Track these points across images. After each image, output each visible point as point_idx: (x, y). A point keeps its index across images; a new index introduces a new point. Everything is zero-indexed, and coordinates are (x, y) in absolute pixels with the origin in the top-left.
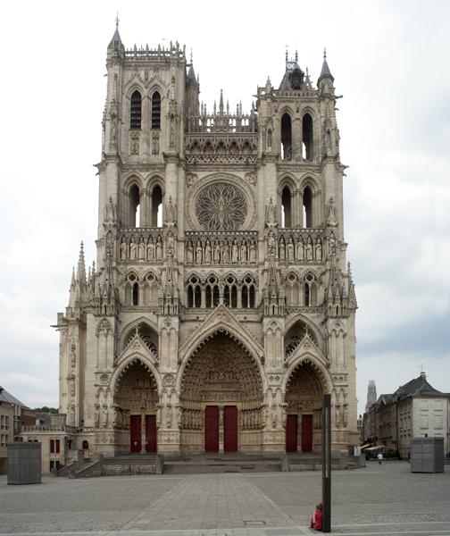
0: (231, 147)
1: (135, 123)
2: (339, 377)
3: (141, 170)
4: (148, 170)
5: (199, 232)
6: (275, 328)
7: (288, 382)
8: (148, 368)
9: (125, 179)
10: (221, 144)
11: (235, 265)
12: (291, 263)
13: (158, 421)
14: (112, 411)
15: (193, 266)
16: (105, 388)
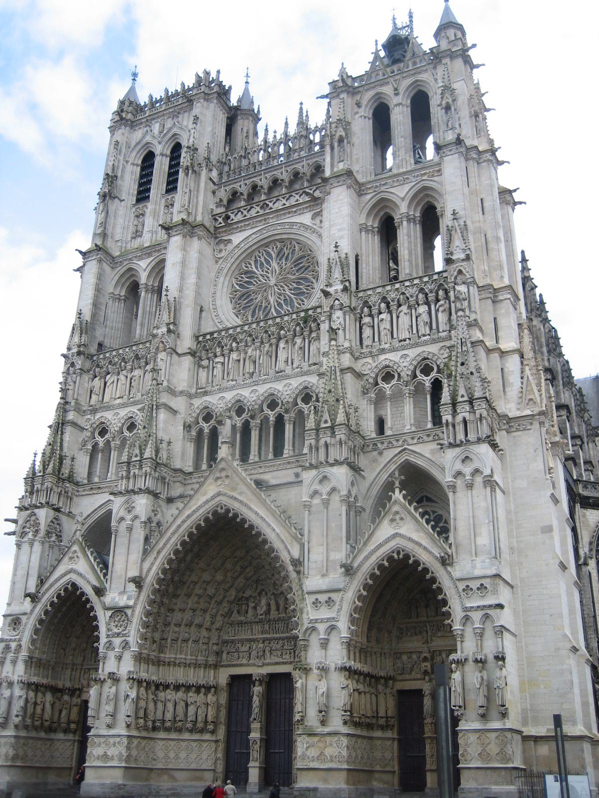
0: (292, 183)
1: (143, 195)
2: (474, 585)
3: (140, 258)
4: (149, 255)
5: (219, 332)
6: (325, 489)
7: (356, 609)
8: (88, 600)
9: (116, 278)
10: (276, 183)
11: (280, 375)
12: (383, 351)
13: (90, 712)
14: (18, 691)
15: (206, 393)
16: (13, 645)
